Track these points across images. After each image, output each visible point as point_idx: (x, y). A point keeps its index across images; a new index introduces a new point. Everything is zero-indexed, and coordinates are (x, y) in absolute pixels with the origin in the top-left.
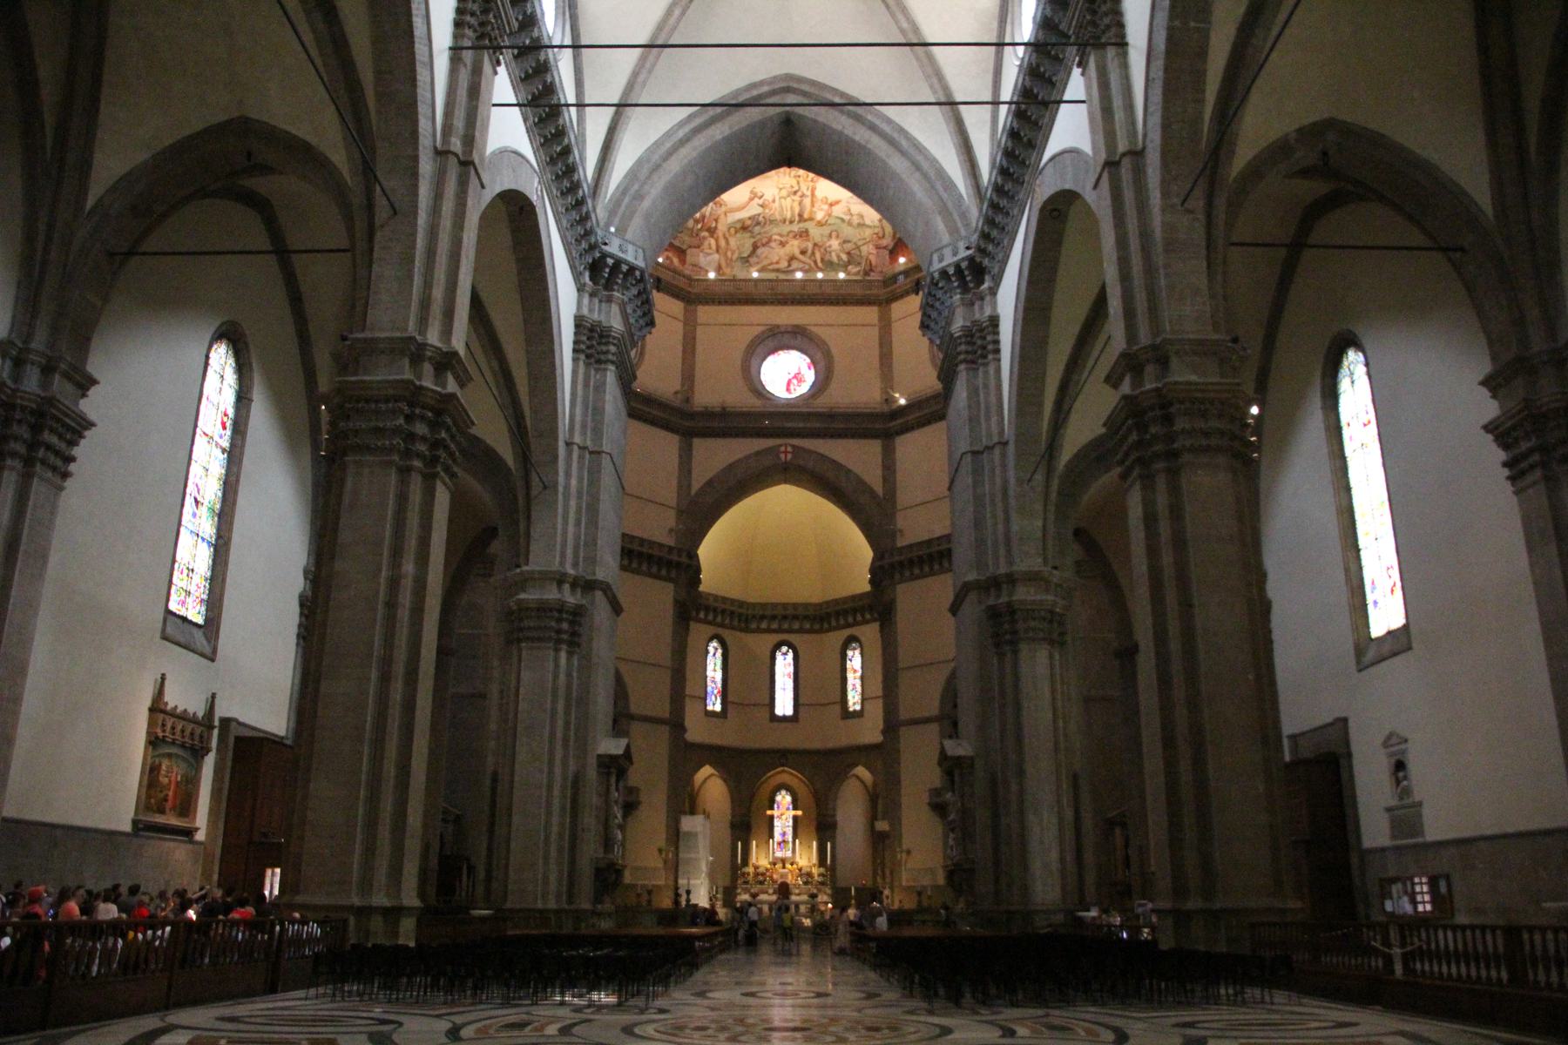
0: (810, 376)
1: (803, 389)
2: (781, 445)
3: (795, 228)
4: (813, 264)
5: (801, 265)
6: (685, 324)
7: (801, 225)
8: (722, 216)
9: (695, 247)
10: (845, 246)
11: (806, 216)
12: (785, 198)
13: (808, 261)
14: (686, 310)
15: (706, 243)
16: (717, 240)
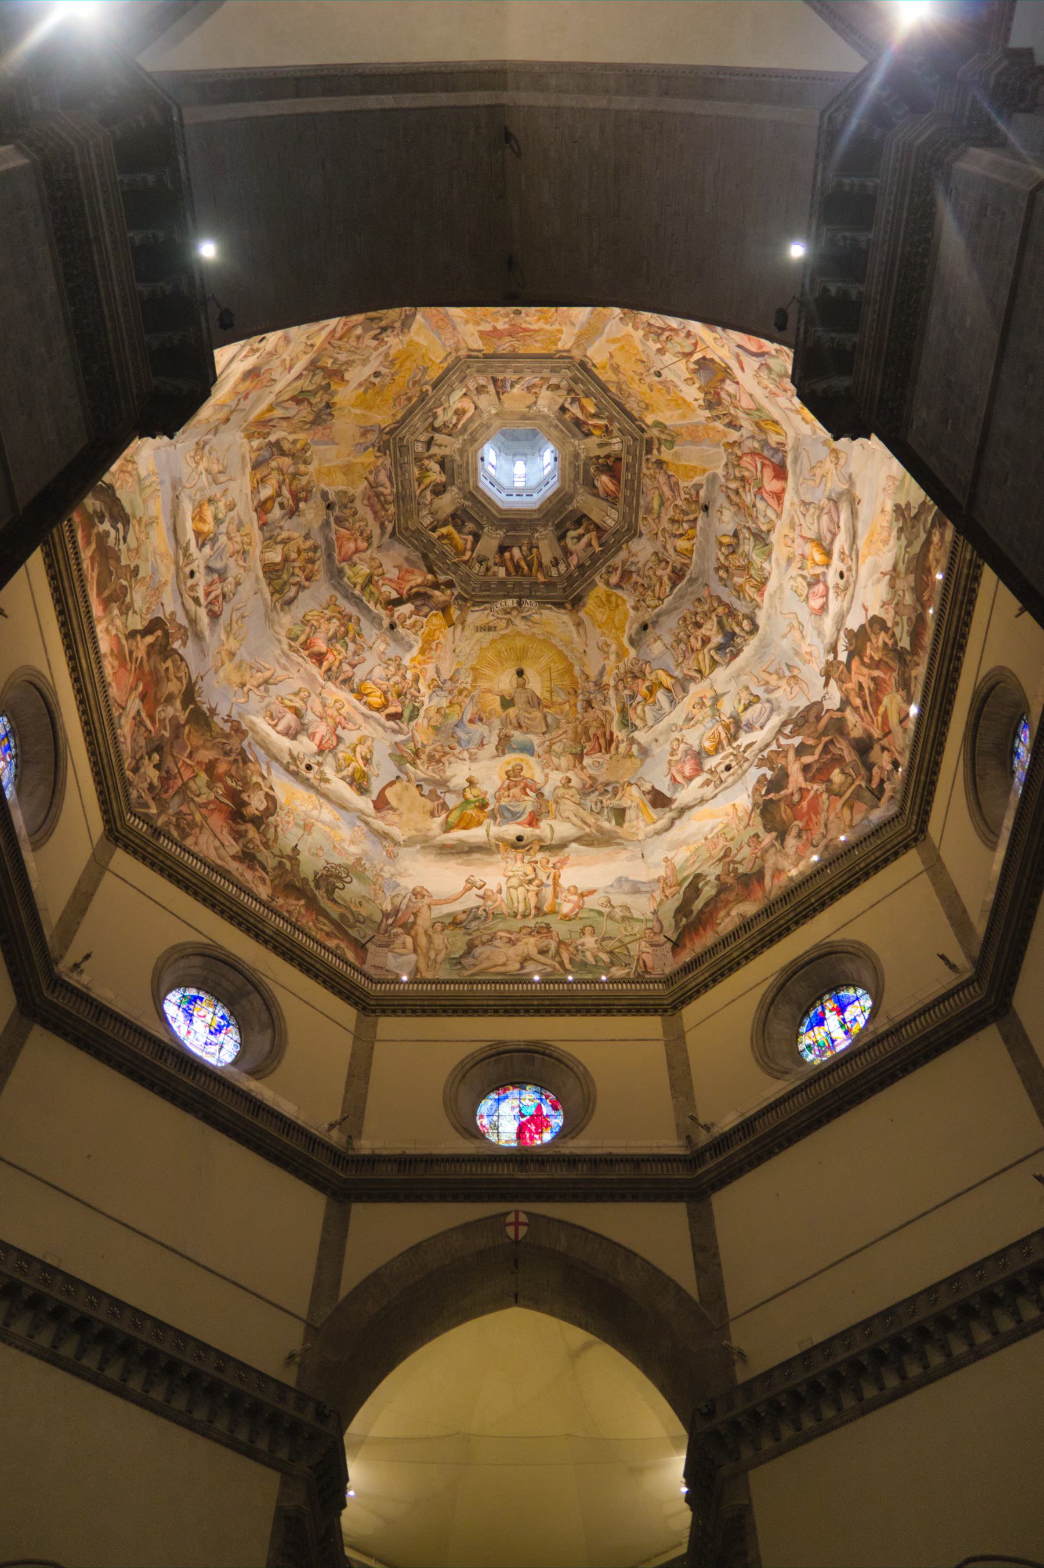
0: (557, 1121)
1: (547, 1137)
2: (508, 1213)
3: (531, 923)
4: (558, 966)
5: (540, 967)
6: (355, 1037)
7: (539, 920)
8: (425, 910)
9: (380, 946)
10: (604, 943)
11: (546, 908)
12: (516, 889)
13: (549, 961)
14: (359, 1021)
15: (399, 941)
16: (415, 939)
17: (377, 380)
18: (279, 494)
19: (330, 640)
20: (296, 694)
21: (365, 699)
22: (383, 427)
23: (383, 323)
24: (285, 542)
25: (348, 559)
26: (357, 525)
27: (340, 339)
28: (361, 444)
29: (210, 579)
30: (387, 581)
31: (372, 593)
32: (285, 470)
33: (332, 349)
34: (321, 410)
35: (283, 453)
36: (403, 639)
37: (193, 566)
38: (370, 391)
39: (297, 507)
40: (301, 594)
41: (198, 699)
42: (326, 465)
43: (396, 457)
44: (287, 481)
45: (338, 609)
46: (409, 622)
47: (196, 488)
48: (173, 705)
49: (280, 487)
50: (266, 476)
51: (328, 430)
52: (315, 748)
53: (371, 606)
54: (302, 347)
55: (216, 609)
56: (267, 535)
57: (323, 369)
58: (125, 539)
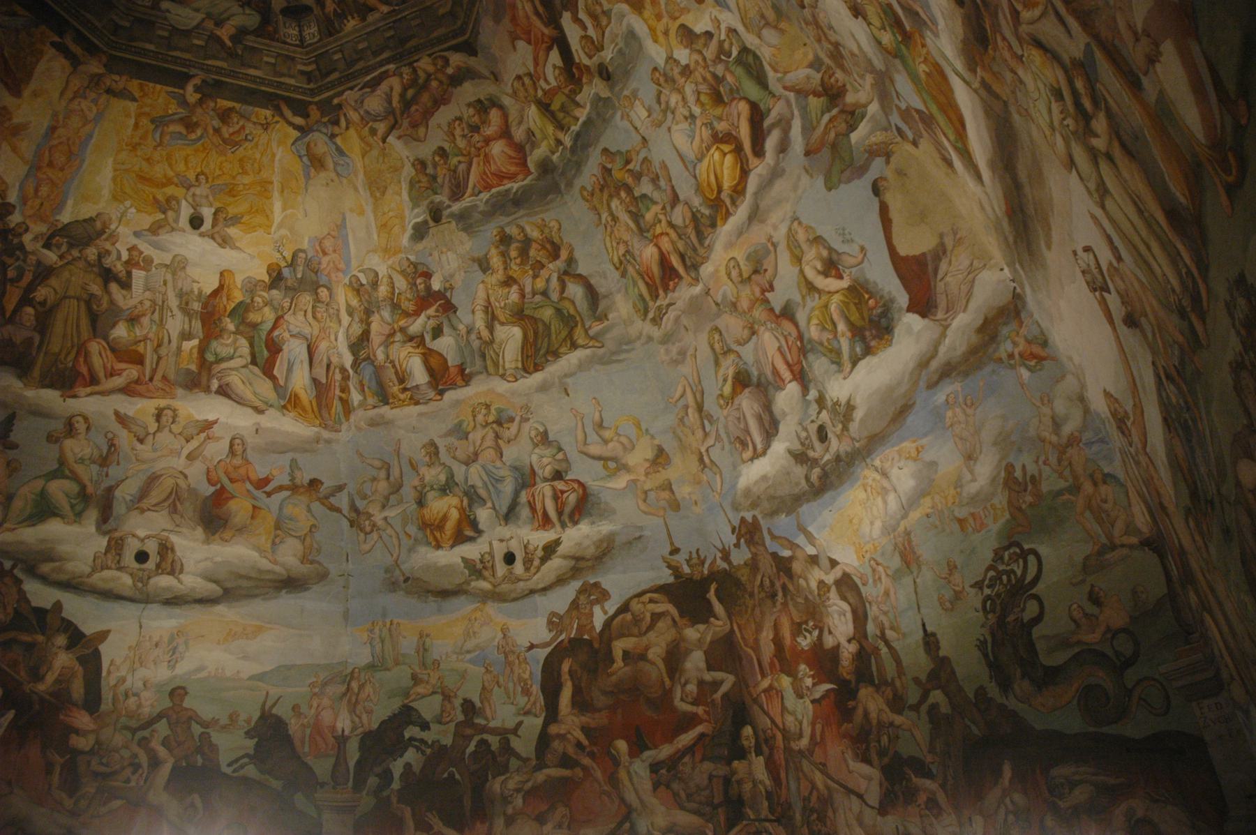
17: (207, 213)
18: (417, 340)
19: (641, 231)
20: (717, 363)
21: (725, 196)
22: (296, 134)
23: (96, 289)
24: (492, 320)
25: (520, 151)
26: (462, 143)
27: (139, 360)
28: (336, 164)
29: (525, 512)
30: (540, 69)
31: (563, 108)
32: (387, 330)
33: (163, 363)
34: (287, 288)
35: (365, 336)
36: (620, 51)
37: (499, 551)
38: (232, 211)
39: (440, 295)
40: (582, 269)
41: (706, 572)
42: (375, 237)
43: (340, 82)
44: (402, 323)
45: (597, 190)
46: (591, 32)
47: (402, 536)
48: (688, 652)
49: (411, 339)
50: (396, 373)
51: (328, 244)
52: (793, 388)
53: (582, 114)
54: (164, 438)
55: (572, 499)
56: (478, 362)
57: (202, 349)
58: (425, 726)
